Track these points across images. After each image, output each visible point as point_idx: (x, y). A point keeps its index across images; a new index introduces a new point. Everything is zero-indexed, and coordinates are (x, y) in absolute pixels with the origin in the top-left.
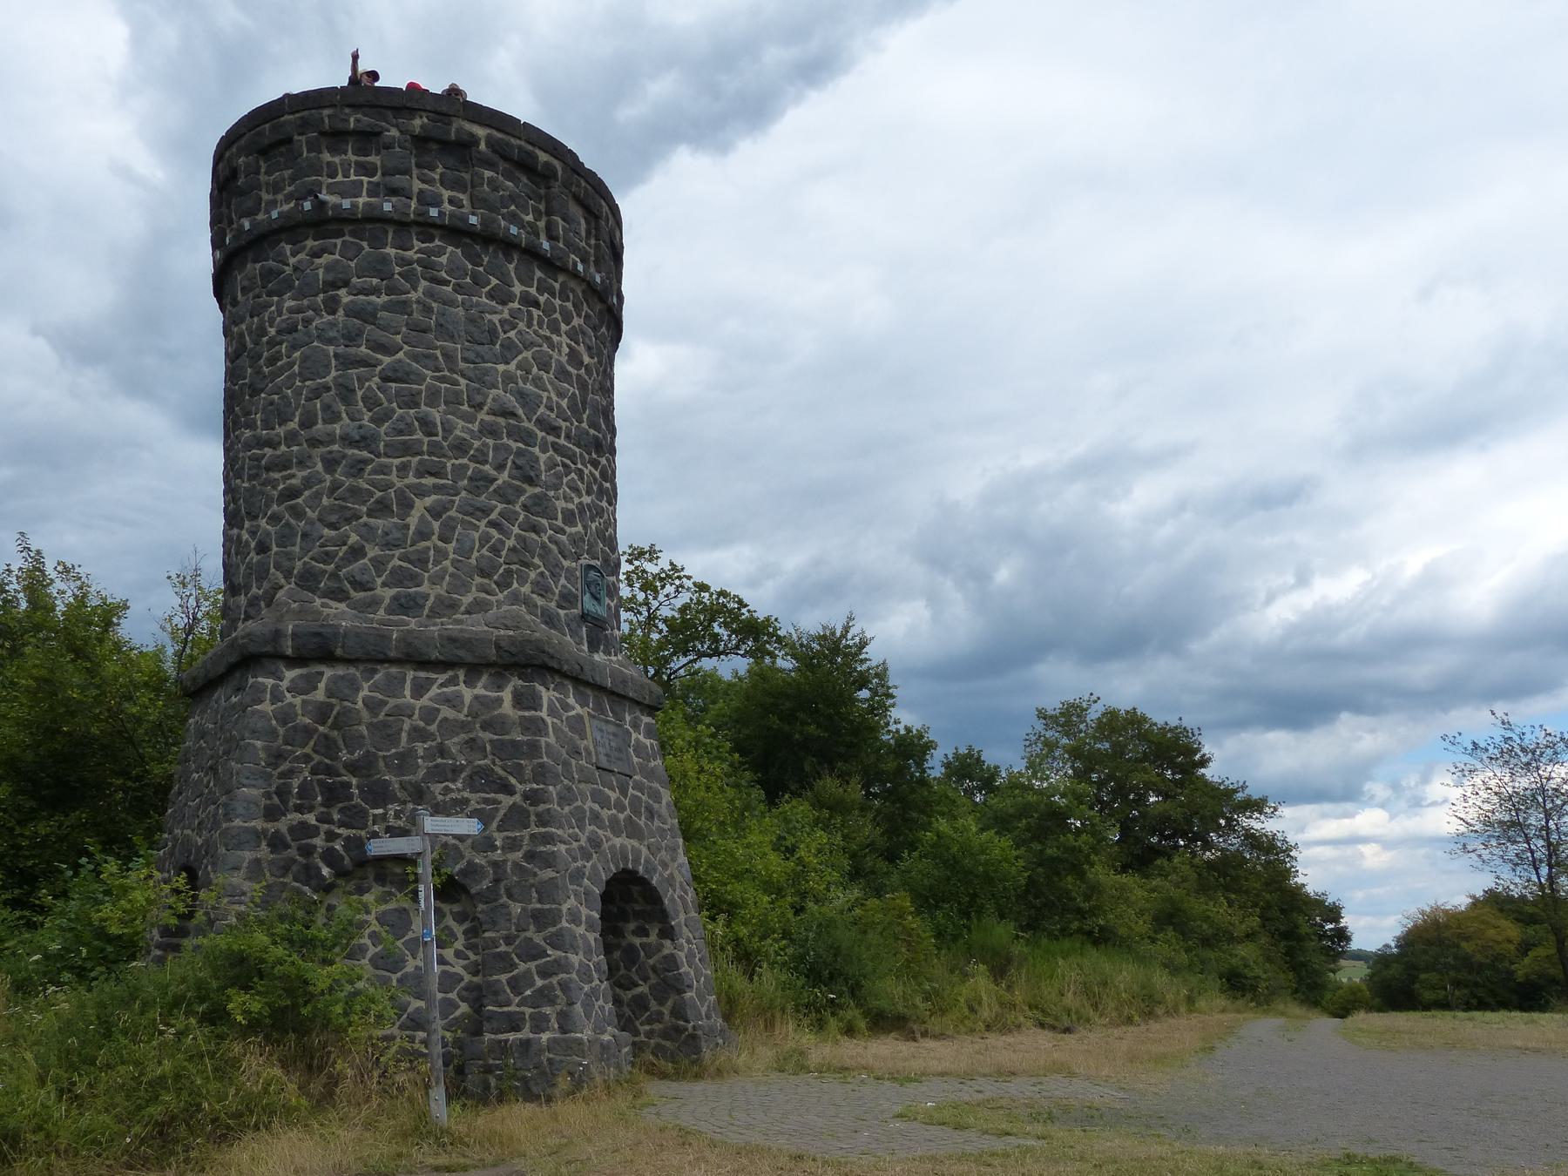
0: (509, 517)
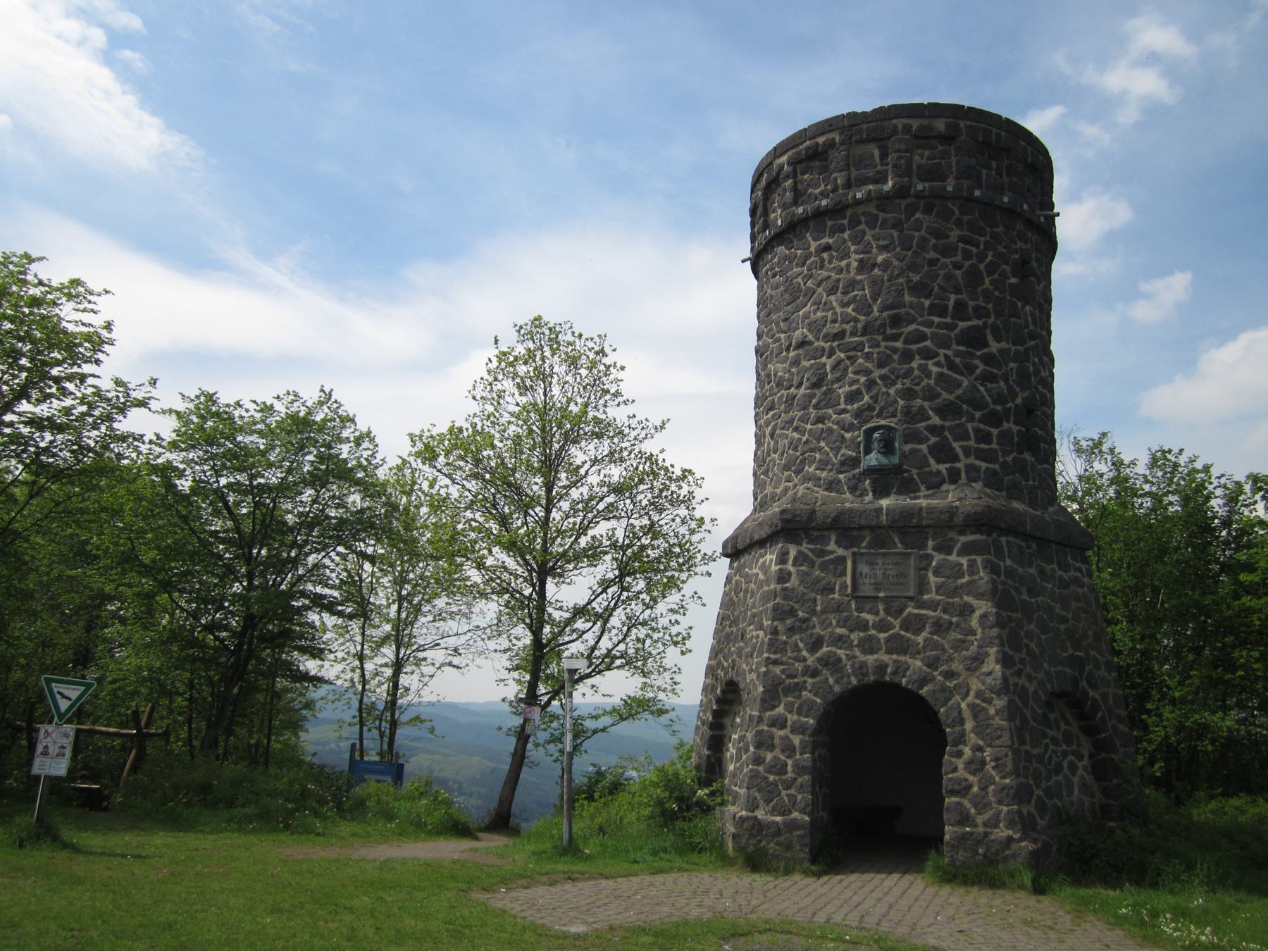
0: (804, 419)
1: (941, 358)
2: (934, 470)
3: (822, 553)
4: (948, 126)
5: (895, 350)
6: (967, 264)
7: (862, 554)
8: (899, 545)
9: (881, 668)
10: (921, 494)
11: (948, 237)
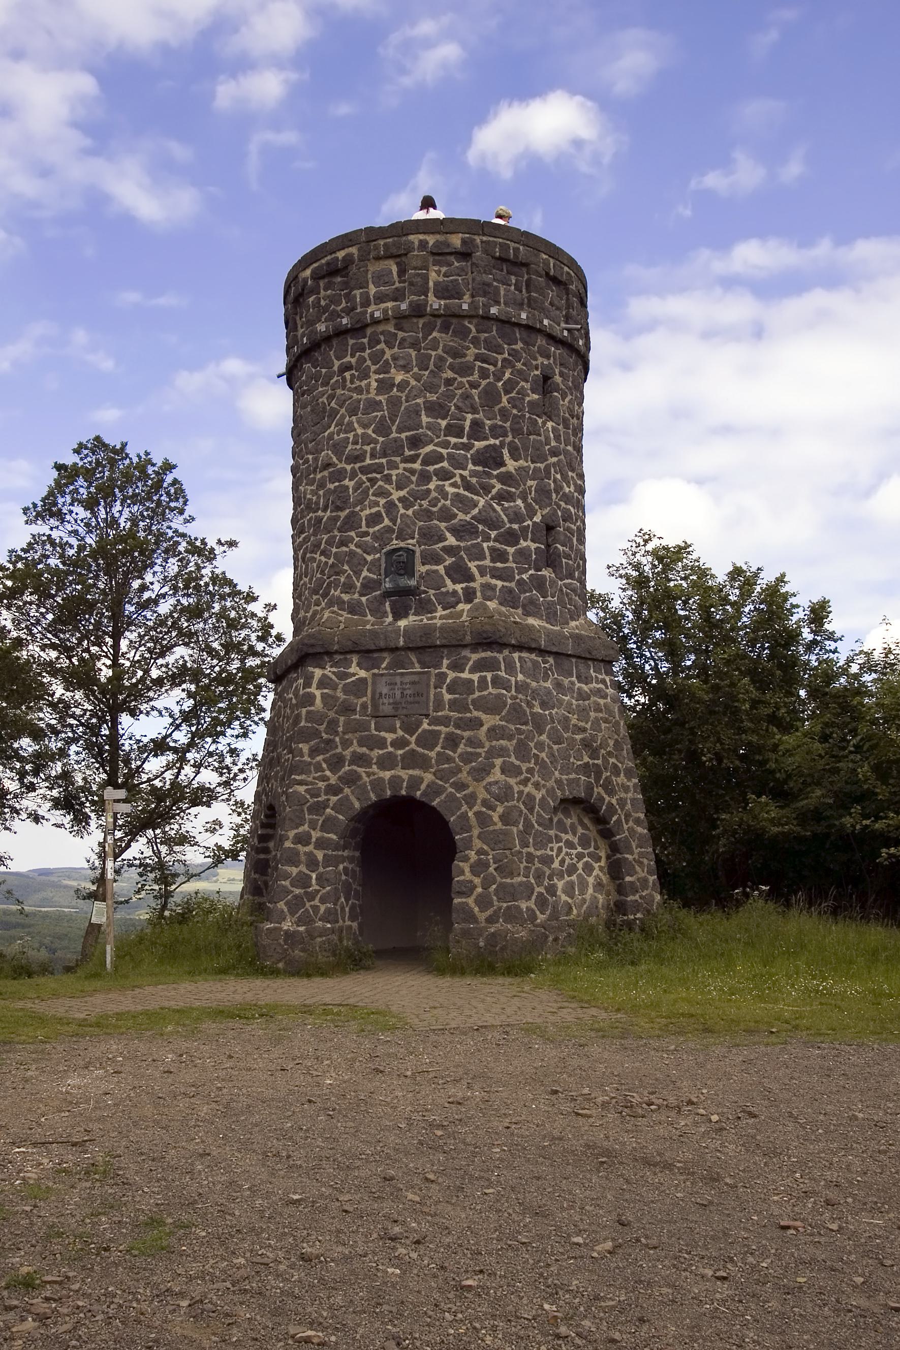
0: (330, 543)
1: (458, 479)
2: (451, 590)
3: (343, 676)
4: (464, 242)
5: (412, 472)
6: (484, 383)
7: (382, 675)
8: (417, 665)
9: (395, 782)
10: (438, 614)
11: (465, 355)
